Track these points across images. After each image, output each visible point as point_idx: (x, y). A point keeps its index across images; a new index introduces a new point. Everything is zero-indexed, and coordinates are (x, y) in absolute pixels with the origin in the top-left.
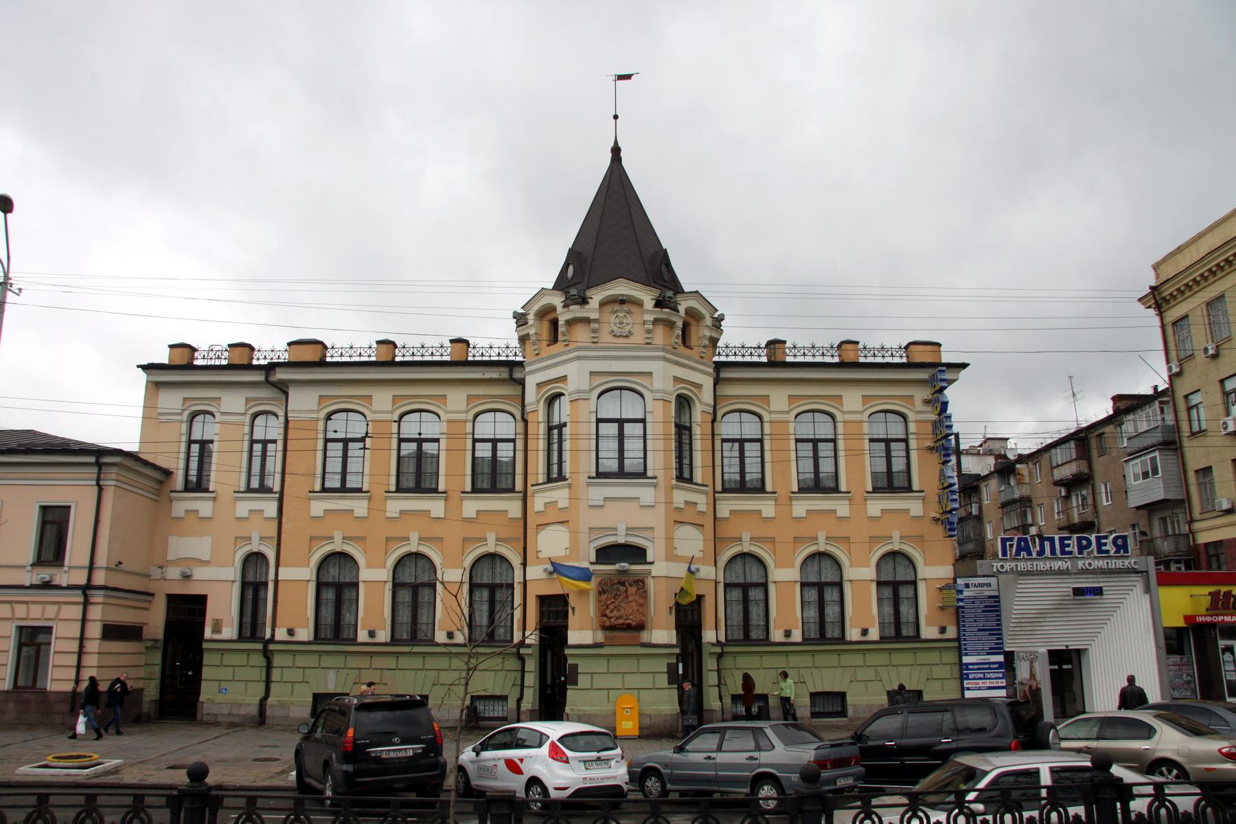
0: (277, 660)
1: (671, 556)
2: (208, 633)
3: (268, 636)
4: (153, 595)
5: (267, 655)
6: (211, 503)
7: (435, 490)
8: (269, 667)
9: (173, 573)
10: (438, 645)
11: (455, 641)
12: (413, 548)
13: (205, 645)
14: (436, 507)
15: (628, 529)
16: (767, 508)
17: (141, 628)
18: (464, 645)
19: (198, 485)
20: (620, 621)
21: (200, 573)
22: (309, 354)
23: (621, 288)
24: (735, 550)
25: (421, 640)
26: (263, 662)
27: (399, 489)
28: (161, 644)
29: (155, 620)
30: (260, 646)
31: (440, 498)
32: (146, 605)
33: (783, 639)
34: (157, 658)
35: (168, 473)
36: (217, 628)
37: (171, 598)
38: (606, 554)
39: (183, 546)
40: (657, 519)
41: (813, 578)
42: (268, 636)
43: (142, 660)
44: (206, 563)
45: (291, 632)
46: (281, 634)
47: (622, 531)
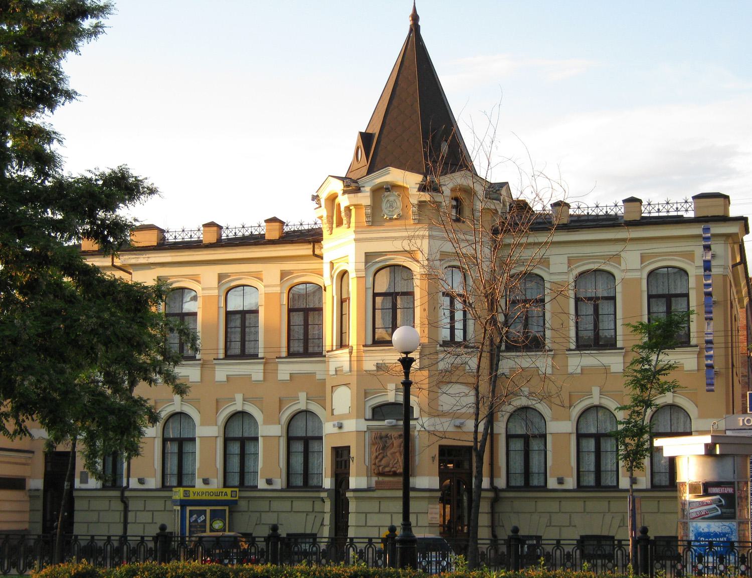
0: (132, 506)
1: (434, 412)
3: (125, 484)
5: (124, 501)
7: (255, 356)
8: (126, 510)
12: (302, 406)
13: (75, 494)
14: (255, 371)
18: (282, 490)
23: (394, 175)
25: (247, 487)
26: (120, 507)
27: (227, 356)
28: (41, 494)
30: (117, 493)
31: (259, 363)
41: (520, 431)
42: (125, 484)
45: (141, 481)
46: (134, 483)
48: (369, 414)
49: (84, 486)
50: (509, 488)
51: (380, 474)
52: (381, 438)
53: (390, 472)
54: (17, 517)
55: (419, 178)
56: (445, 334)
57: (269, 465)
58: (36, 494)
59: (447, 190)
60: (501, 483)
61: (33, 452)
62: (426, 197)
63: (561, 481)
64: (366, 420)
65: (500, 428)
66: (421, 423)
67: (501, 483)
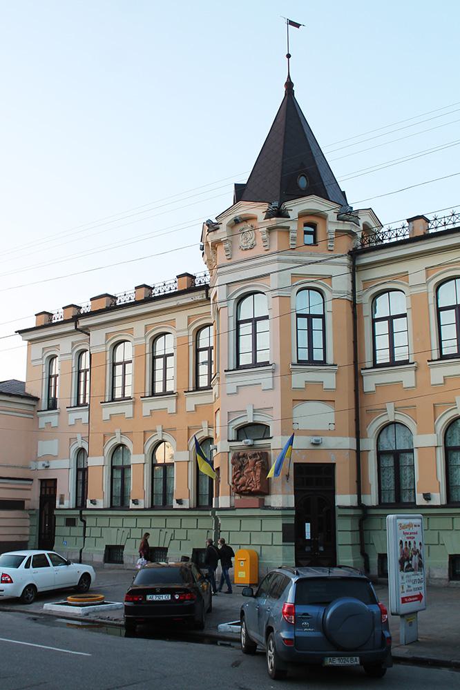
2: (58, 505)
4: (32, 480)
6: (57, 416)
9: (40, 465)
10: (273, 509)
11: (431, 503)
15: (254, 411)
16: (406, 377)
17: (24, 502)
19: (52, 405)
20: (243, 488)
21: (54, 464)
22: (103, 304)
24: (383, 420)
29: (33, 496)
32: (29, 487)
33: (424, 503)
34: (36, 521)
35: (37, 399)
36: (62, 503)
37: (42, 481)
38: (243, 431)
39: (48, 447)
40: (274, 400)
43: (28, 523)
44: (55, 457)
47: (250, 412)
48: (233, 436)
49: (62, 506)
50: (381, 505)
51: (240, 493)
52: (239, 458)
53: (246, 490)
54: (20, 531)
55: (265, 207)
56: (304, 356)
57: (139, 487)
58: (34, 512)
59: (293, 214)
60: (371, 499)
61: (32, 480)
62: (274, 221)
63: (427, 497)
64: (229, 441)
65: (369, 444)
66: (276, 442)
67: (371, 499)
